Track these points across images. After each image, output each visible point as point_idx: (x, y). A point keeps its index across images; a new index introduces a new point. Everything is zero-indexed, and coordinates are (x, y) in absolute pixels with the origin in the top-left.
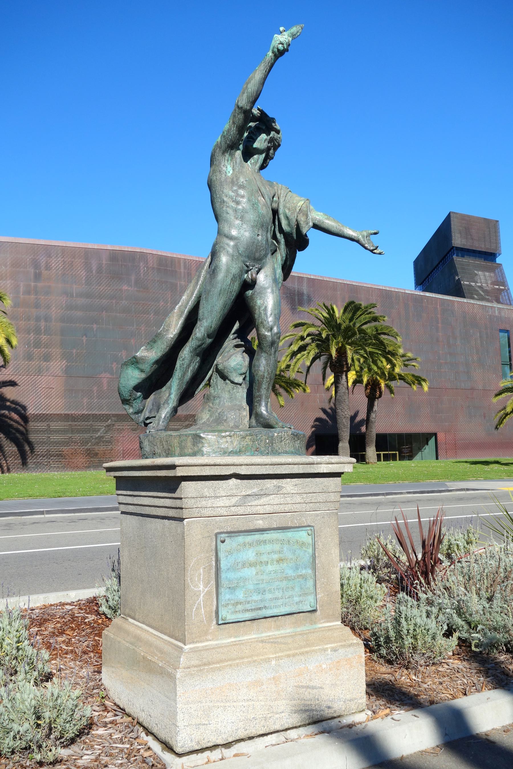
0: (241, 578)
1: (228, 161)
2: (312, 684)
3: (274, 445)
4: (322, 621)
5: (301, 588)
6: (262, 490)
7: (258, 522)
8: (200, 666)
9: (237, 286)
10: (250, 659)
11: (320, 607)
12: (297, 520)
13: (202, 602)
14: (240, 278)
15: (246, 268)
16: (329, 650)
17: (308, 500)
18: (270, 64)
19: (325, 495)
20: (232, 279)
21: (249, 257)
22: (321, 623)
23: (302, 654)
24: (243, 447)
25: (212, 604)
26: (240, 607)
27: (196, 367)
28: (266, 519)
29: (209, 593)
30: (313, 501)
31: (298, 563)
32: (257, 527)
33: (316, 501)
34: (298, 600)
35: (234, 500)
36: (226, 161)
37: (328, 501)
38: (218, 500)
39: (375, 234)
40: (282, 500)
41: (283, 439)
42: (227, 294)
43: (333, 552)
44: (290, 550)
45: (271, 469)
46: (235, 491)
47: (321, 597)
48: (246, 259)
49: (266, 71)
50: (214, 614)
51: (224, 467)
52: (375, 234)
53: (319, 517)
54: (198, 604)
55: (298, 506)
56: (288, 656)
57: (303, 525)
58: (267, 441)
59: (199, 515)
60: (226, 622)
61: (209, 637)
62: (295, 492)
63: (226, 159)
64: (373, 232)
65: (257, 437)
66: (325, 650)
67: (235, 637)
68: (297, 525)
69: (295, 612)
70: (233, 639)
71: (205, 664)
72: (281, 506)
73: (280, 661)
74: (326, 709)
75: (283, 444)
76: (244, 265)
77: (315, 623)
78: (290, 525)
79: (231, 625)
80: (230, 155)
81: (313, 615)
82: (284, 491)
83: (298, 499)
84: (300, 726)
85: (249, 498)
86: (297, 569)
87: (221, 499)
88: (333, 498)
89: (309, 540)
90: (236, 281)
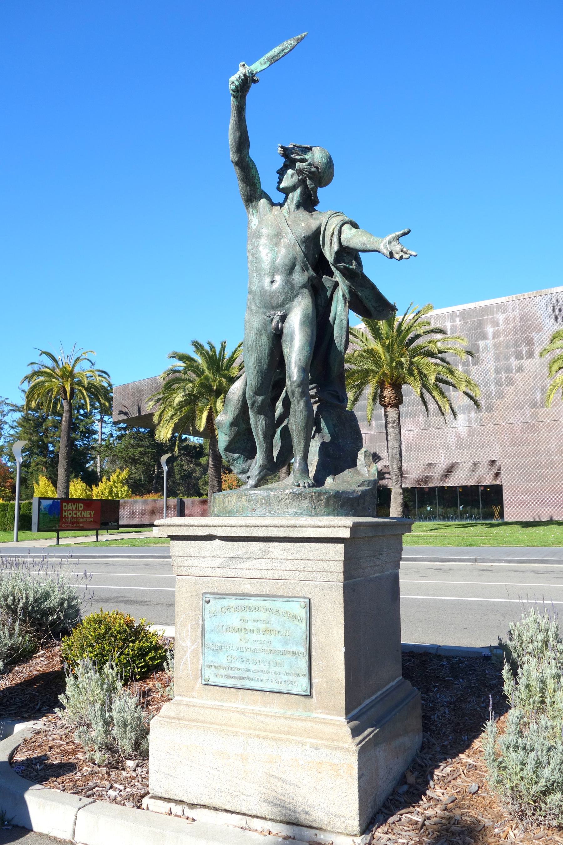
0: (224, 642)
1: (253, 214)
2: (284, 777)
3: (272, 505)
4: (319, 711)
5: (291, 667)
6: (246, 553)
7: (246, 586)
8: (174, 718)
9: (266, 339)
10: (219, 727)
11: (316, 693)
12: (290, 589)
13: (189, 659)
14: (266, 331)
15: (268, 319)
16: (308, 746)
17: (301, 568)
18: (234, 108)
19: (322, 564)
20: (256, 334)
21: (265, 307)
22: (318, 713)
23: (274, 739)
24: (240, 507)
25: (198, 662)
26: (222, 672)
27: (264, 425)
28: (255, 584)
29: (195, 651)
30: (307, 569)
31: (288, 638)
32: (245, 592)
33: (311, 569)
34: (287, 680)
35: (218, 562)
36: (252, 216)
37: (326, 570)
38: (203, 560)
39: (405, 234)
40: (270, 565)
41: (280, 498)
42: (257, 349)
43: (335, 632)
44: (278, 622)
45: (247, 532)
46: (218, 553)
47: (319, 682)
48: (265, 310)
49: (234, 116)
50: (200, 673)
51: (199, 528)
52: (405, 234)
53: (318, 589)
54: (186, 659)
55: (290, 573)
56: (258, 737)
57: (297, 595)
58: (264, 501)
59: (186, 574)
60: (209, 683)
61: (194, 694)
62: (284, 557)
63: (251, 213)
64: (401, 232)
65: (252, 497)
66: (303, 744)
67: (220, 701)
68: (290, 595)
69: (282, 691)
70: (217, 703)
71: (179, 719)
72: (270, 572)
73: (248, 739)
74: (302, 813)
75: (283, 503)
76: (265, 317)
77: (310, 710)
78: (281, 593)
79: (215, 687)
80: (253, 208)
81: (307, 701)
82: (271, 555)
83: (289, 565)
84: (270, 820)
85: (234, 561)
86: (286, 643)
87: (206, 559)
88: (333, 567)
89: (303, 613)
90: (262, 334)
